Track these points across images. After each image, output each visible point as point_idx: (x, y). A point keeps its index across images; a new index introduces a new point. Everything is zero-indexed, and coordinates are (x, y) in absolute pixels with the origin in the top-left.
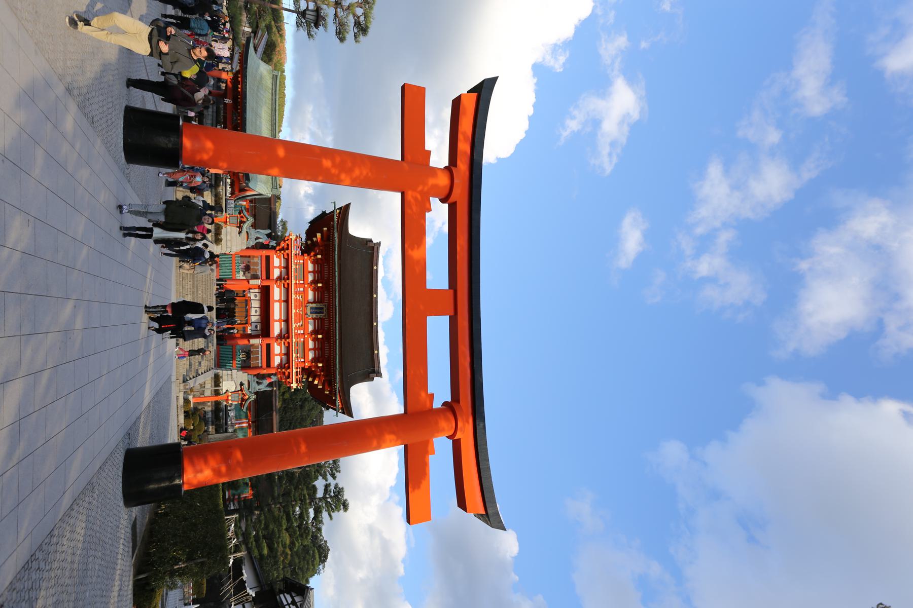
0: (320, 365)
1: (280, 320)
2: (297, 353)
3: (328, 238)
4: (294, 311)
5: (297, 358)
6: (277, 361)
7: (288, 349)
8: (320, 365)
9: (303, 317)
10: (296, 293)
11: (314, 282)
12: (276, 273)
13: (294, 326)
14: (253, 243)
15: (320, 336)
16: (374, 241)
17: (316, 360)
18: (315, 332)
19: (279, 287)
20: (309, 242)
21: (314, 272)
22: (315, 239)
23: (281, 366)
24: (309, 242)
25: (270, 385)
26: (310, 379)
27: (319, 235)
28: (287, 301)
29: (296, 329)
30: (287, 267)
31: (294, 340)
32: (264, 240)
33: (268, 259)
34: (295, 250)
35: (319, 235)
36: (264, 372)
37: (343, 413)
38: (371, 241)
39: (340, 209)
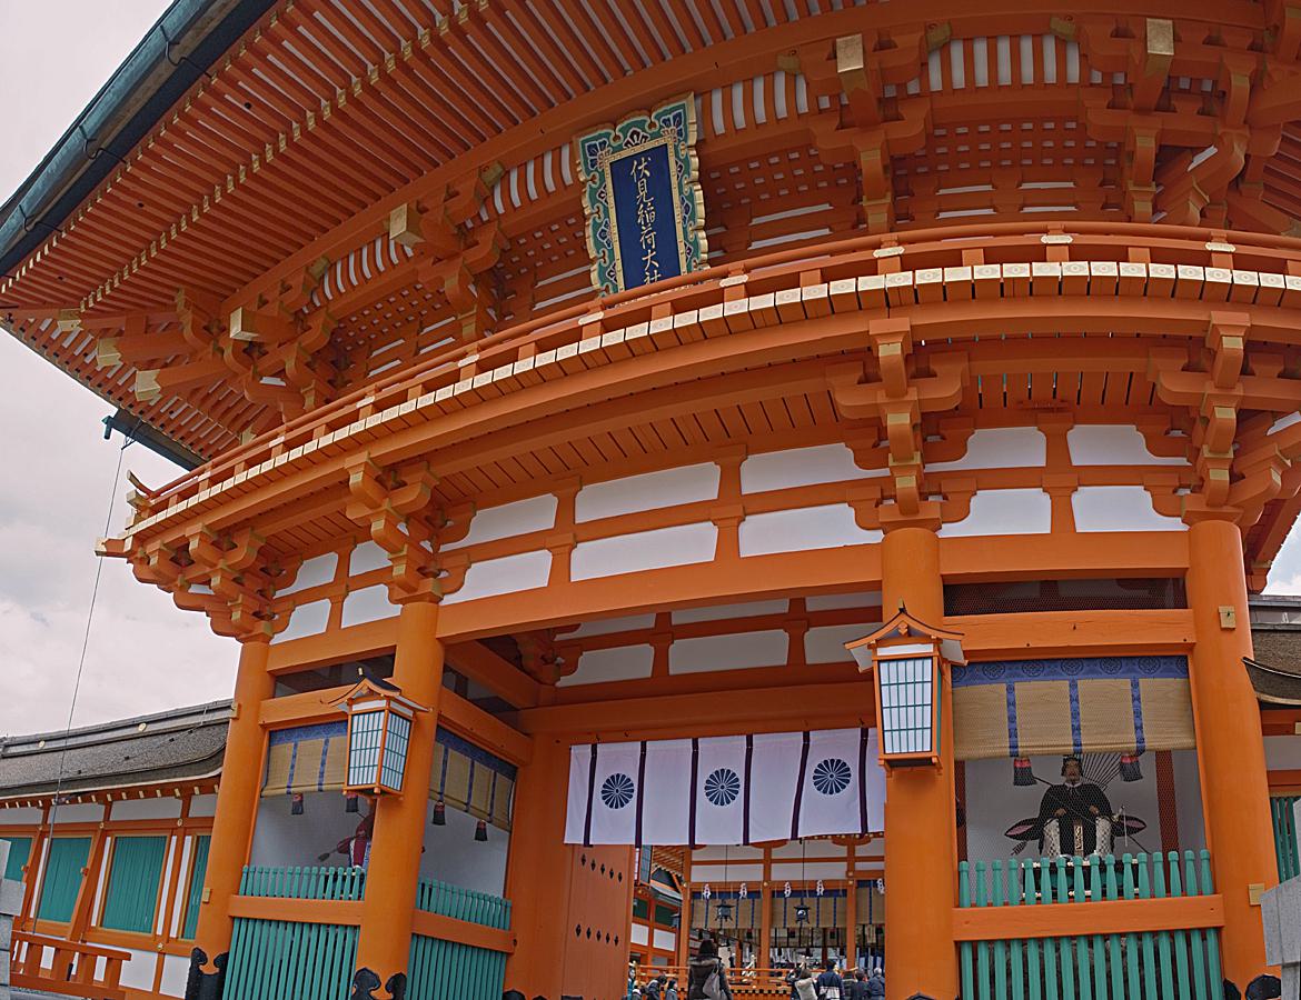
1: (730, 509)
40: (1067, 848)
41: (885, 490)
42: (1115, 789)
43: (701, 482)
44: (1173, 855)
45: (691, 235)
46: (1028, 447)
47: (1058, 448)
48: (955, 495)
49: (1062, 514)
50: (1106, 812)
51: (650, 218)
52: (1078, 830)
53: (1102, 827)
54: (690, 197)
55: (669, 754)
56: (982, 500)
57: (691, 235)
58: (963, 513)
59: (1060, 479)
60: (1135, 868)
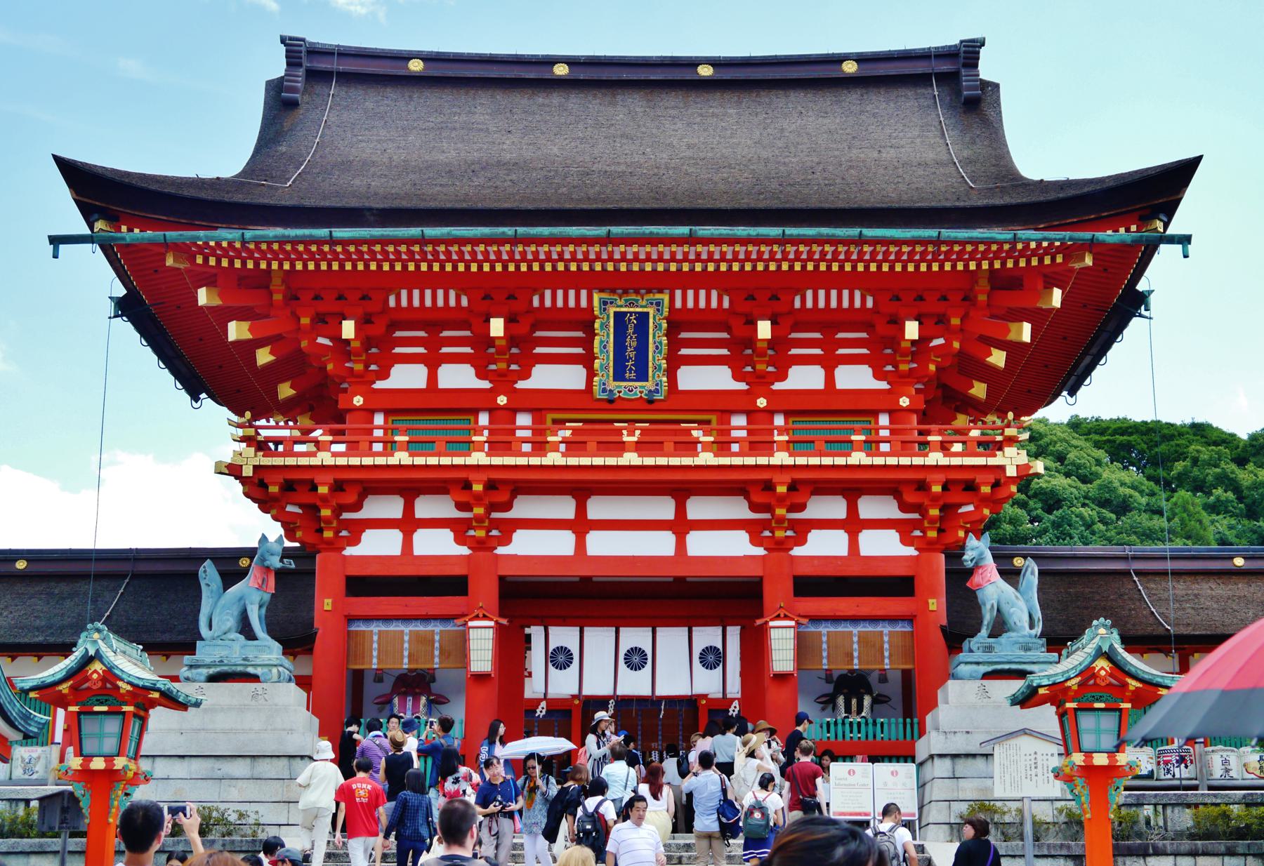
0: (912, 330)
1: (681, 526)
2: (847, 446)
3: (248, 289)
4: (631, 458)
5: (871, 445)
6: (882, 545)
7: (824, 484)
8: (912, 330)
10: (540, 447)
11: (482, 354)
12: (436, 544)
13: (706, 458)
14: (268, 652)
15: (764, 329)
16: (278, 68)
17: (882, 350)
18: (740, 353)
20: (285, 391)
21: (433, 362)
22: (264, 357)
24: (285, 391)
25: (1011, 575)
26: (979, 390)
27: (236, 331)
28: (580, 487)
29: (722, 447)
30: (409, 486)
31: (781, 458)
32: (252, 593)
34: (334, 455)
35: (236, 331)
37: (1169, 210)
38: (275, 89)
39: (89, 213)
40: (848, 710)
41: (764, 524)
43: (663, 508)
44: (908, 720)
45: (657, 359)
46: (835, 508)
47: (852, 509)
48: (802, 529)
49: (854, 544)
51: (634, 344)
52: (854, 701)
54: (657, 338)
56: (814, 535)
57: (657, 359)
60: (882, 724)
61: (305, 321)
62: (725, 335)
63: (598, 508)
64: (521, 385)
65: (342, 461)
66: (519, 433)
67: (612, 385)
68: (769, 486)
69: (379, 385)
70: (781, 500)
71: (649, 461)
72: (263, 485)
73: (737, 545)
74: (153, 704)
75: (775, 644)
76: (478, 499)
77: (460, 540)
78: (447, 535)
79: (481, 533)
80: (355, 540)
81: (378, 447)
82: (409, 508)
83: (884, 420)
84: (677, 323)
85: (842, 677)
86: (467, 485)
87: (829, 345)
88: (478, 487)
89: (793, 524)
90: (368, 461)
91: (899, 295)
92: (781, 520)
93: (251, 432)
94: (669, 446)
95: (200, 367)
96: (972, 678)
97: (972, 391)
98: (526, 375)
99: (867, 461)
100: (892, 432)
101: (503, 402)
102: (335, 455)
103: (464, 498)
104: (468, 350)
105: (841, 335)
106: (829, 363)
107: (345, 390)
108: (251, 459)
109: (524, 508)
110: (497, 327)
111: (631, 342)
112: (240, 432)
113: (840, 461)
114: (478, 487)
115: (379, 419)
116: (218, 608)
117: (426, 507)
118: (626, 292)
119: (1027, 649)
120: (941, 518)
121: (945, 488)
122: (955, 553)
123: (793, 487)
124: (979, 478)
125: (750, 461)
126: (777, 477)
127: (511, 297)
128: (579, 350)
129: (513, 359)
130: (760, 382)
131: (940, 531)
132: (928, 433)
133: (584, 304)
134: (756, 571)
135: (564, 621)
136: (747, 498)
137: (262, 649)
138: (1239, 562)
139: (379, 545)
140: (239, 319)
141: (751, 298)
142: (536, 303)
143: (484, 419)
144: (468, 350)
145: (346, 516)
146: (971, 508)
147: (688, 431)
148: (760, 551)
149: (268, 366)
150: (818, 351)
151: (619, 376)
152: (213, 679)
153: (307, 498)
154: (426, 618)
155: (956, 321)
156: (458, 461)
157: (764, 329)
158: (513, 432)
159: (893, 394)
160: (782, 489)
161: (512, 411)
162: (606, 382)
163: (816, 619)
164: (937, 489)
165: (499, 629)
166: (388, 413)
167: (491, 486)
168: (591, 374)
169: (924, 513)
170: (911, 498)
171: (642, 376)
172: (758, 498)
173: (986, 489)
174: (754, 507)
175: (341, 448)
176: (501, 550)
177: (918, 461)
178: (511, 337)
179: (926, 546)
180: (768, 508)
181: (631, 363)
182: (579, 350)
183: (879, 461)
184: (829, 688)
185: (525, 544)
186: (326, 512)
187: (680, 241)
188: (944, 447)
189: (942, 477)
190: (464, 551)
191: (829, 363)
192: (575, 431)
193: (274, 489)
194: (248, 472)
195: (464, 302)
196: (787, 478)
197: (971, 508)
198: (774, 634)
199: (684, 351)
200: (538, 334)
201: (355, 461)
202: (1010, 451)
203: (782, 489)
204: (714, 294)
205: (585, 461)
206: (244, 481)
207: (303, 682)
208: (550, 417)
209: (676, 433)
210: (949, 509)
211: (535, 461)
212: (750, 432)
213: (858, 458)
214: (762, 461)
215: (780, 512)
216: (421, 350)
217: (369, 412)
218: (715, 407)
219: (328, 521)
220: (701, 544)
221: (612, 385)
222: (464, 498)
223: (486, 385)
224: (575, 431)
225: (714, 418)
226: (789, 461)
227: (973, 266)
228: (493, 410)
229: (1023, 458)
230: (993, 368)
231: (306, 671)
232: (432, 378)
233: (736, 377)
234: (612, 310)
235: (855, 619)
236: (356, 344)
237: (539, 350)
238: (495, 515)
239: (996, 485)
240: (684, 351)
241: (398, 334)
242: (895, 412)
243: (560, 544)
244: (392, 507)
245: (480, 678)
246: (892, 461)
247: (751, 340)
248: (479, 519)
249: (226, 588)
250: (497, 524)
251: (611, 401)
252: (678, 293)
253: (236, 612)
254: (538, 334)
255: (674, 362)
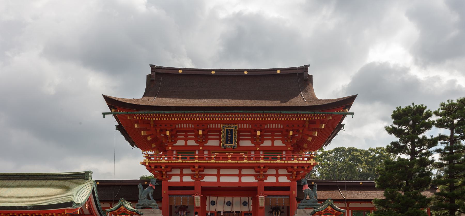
0: (291, 133)
1: (240, 175)
2: (276, 159)
4: (229, 161)
5: (281, 159)
6: (283, 180)
8: (291, 133)
9: (238, 152)
10: (210, 159)
12: (187, 179)
13: (246, 161)
14: (154, 203)
15: (259, 133)
17: (285, 137)
18: (253, 138)
19: (203, 176)
20: (153, 145)
21: (186, 140)
22: (149, 139)
23: (288, 177)
26: (305, 146)
28: (219, 167)
29: (249, 159)
30: (182, 167)
31: (262, 161)
32: (149, 191)
33: (173, 188)
36: (295, 193)
41: (258, 175)
42: (281, 208)
43: (236, 172)
46: (273, 172)
47: (277, 172)
48: (266, 176)
49: (277, 180)
50: (280, 211)
53: (279, 213)
54: (235, 134)
55: (221, 199)
56: (269, 178)
58: (266, 179)
59: (277, 175)
61: (158, 131)
62: (250, 134)
63: (222, 171)
64: (205, 145)
65: (167, 162)
66: (205, 156)
67: (225, 145)
68: (259, 167)
69: (175, 145)
70: (262, 170)
71: (233, 162)
72: (150, 167)
73: (252, 180)
74: (134, 214)
75: (260, 201)
76: (197, 170)
77: (192, 178)
78: (190, 177)
79: (197, 177)
80: (170, 178)
81: (174, 159)
82: (182, 172)
83: (284, 153)
84: (239, 131)
85: (274, 207)
86: (194, 167)
87: (273, 136)
88: (197, 167)
89: (264, 175)
90: (173, 162)
91: (288, 126)
92: (262, 174)
93: (147, 155)
94: (238, 158)
95: (133, 139)
96: (302, 208)
97: (304, 146)
98: (207, 143)
99: (281, 162)
100: (286, 156)
101: (202, 148)
102: (166, 160)
103: (193, 169)
104: (194, 137)
105: (275, 134)
106: (273, 140)
107: (167, 146)
108: (148, 161)
109: (206, 171)
110: (200, 132)
111: (229, 135)
112: (145, 155)
113: (275, 162)
114: (197, 167)
115: (175, 152)
116: (142, 193)
117: (185, 171)
118: (228, 124)
119: (314, 202)
120: (296, 174)
121: (297, 168)
122: (299, 182)
123: (264, 167)
124: (305, 166)
125: (255, 162)
126: (261, 165)
127: (203, 125)
128: (218, 137)
129: (204, 139)
130: (257, 144)
131: (296, 177)
132: (294, 156)
133: (219, 127)
134: (256, 185)
135: (214, 196)
136: (254, 169)
137: (153, 202)
138: (361, 183)
139: (175, 179)
140: (143, 130)
141: (256, 126)
142: (209, 127)
143: (197, 152)
144: (194, 137)
145: (168, 173)
146: (303, 172)
147: (242, 155)
148: (257, 181)
149: (150, 141)
150: (270, 137)
151: (227, 143)
152: (142, 208)
153: (160, 170)
154: (186, 195)
155: (301, 131)
156: (192, 162)
157: (259, 133)
158: (204, 155)
159: (286, 147)
160: (262, 168)
161: (203, 150)
162: (224, 144)
163: (269, 196)
164: (296, 168)
165: (201, 197)
166: (176, 151)
167: (199, 167)
168: (221, 142)
169: (293, 173)
170: (290, 170)
171: (232, 143)
172: (257, 170)
173: (306, 168)
174: (256, 171)
175: (166, 158)
176: (202, 181)
177: (292, 162)
178: (203, 135)
179: (293, 180)
180: (259, 172)
181: (229, 140)
182: (218, 137)
183: (283, 162)
184: (271, 210)
185: (207, 179)
186: (164, 173)
187: (241, 114)
188: (297, 159)
189: (297, 165)
190: (193, 181)
191: (273, 140)
192: (217, 155)
193: (153, 168)
194: (147, 164)
195: (193, 126)
196: (263, 165)
197: (303, 172)
198: (260, 198)
199: (241, 137)
200: (209, 133)
201: (170, 162)
202: (312, 160)
203: (262, 168)
204: (248, 125)
205: (220, 162)
206: (146, 166)
207: (160, 208)
208: (212, 152)
209: (239, 156)
210: (298, 173)
211: (209, 162)
212: (255, 155)
213: (279, 161)
214: (258, 162)
215: (262, 173)
216: (183, 137)
217: (172, 151)
218: (247, 150)
219: (164, 174)
220: (245, 179)
221: (225, 145)
222: (193, 169)
223: (197, 145)
224: (217, 155)
225: (247, 152)
226: (264, 162)
227: (305, 119)
228: (199, 150)
229: (315, 161)
230: (309, 141)
231: (160, 206)
232: (186, 143)
233: (252, 143)
234: (225, 128)
235: (277, 196)
236: (169, 136)
237: (209, 137)
238: (200, 173)
239: (309, 167)
240: (241, 137)
241: (178, 133)
242: (287, 151)
243: (214, 179)
244: (178, 171)
245: (198, 208)
246: (286, 162)
247: (256, 135)
248: (197, 174)
249: (144, 188)
250: (200, 175)
251: (225, 148)
252: (240, 125)
253: (147, 194)
254: (209, 133)
255: (239, 140)
